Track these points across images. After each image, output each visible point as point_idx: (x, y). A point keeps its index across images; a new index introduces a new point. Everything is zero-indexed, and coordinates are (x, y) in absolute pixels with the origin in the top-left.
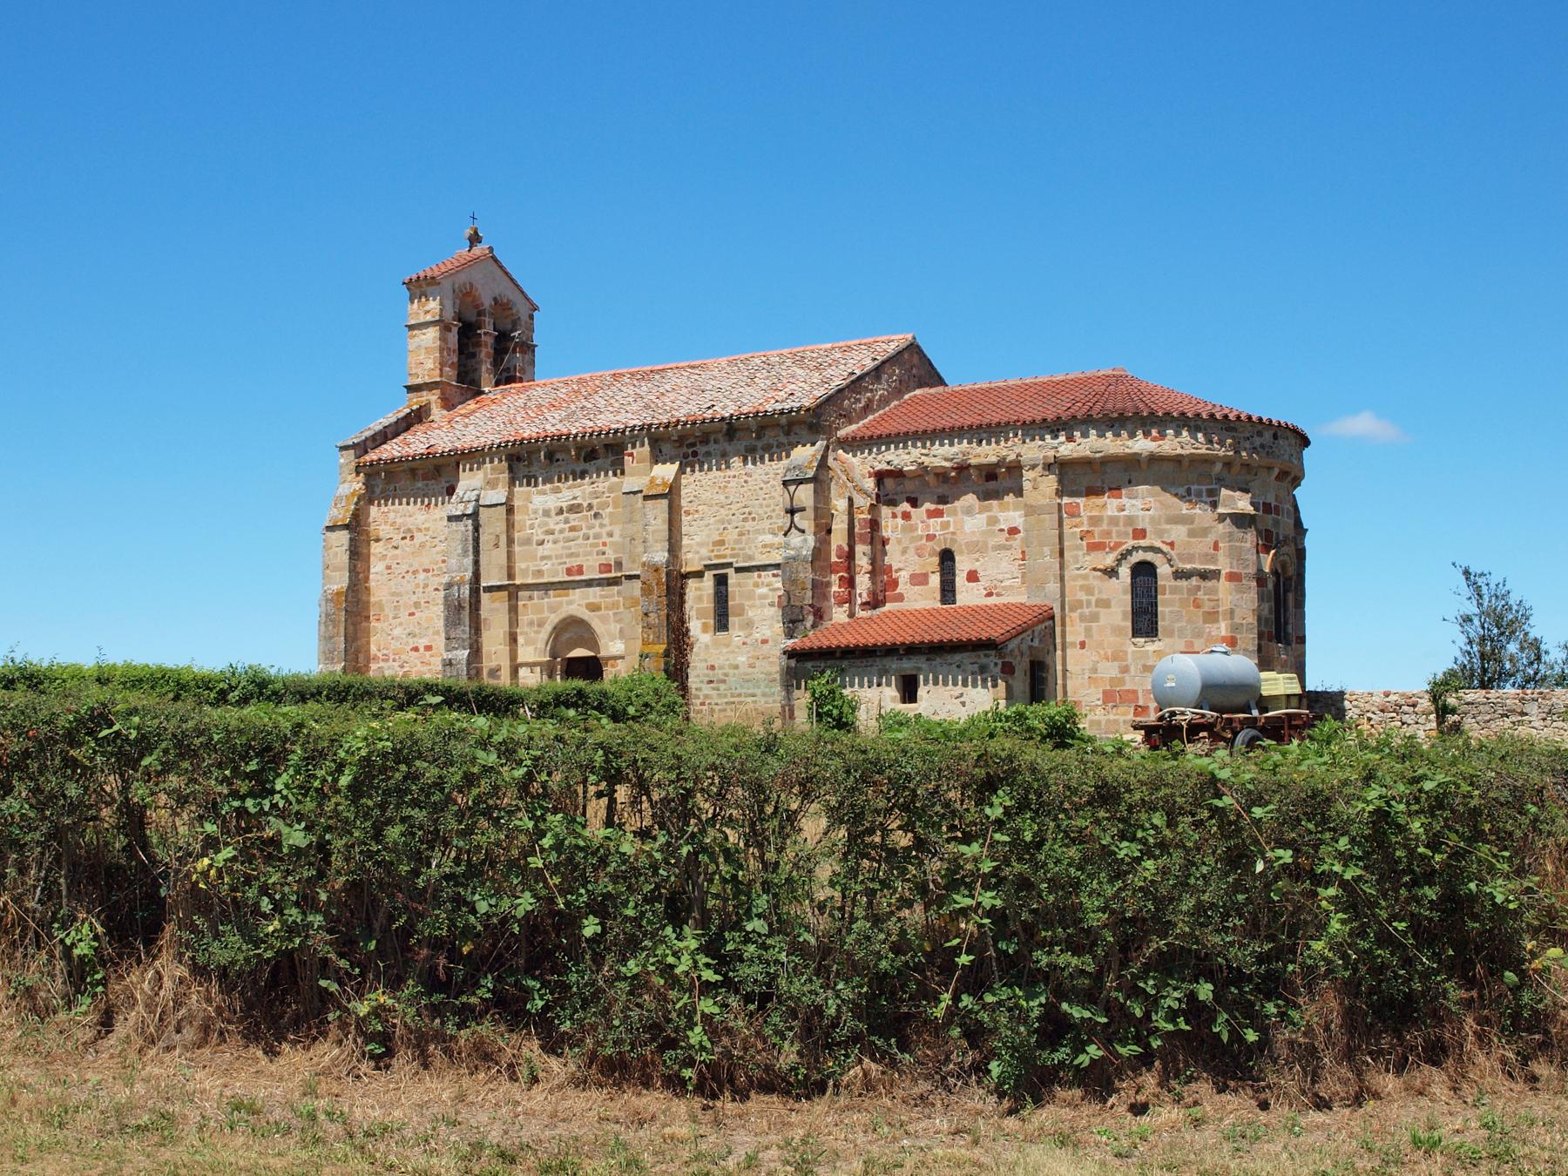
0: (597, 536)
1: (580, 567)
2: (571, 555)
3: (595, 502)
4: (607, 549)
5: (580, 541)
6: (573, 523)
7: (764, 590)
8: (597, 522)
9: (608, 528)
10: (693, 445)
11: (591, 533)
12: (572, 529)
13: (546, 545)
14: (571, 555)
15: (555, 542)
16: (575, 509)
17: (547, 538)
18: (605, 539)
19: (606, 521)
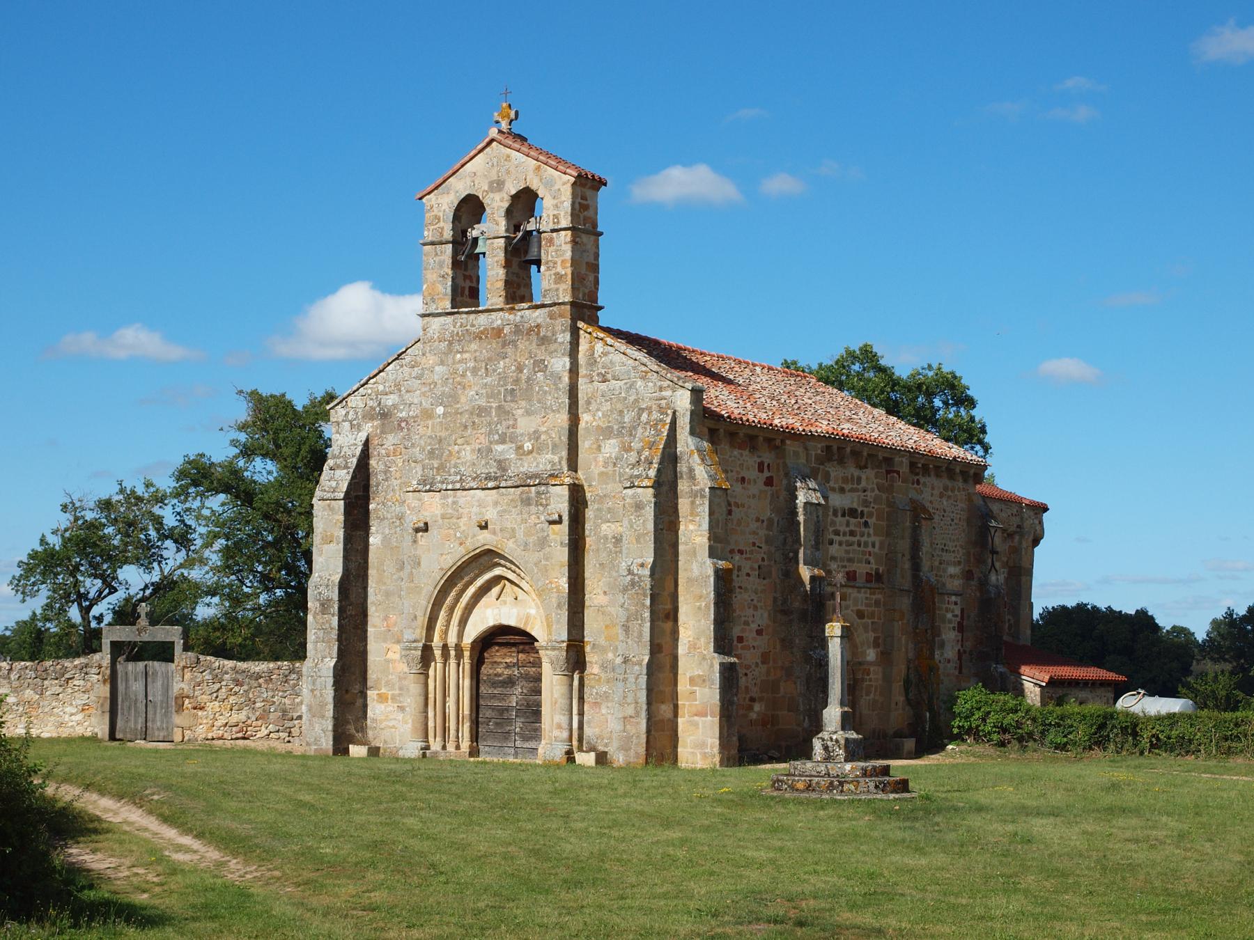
0: (866, 544)
1: (855, 572)
2: (850, 560)
3: (866, 510)
4: (872, 560)
5: (856, 547)
6: (852, 528)
7: (949, 616)
8: (866, 530)
9: (873, 539)
10: (917, 474)
11: (863, 539)
12: (852, 533)
13: (836, 546)
14: (850, 560)
15: (840, 544)
16: (852, 513)
17: (836, 538)
18: (870, 549)
19: (871, 531)
